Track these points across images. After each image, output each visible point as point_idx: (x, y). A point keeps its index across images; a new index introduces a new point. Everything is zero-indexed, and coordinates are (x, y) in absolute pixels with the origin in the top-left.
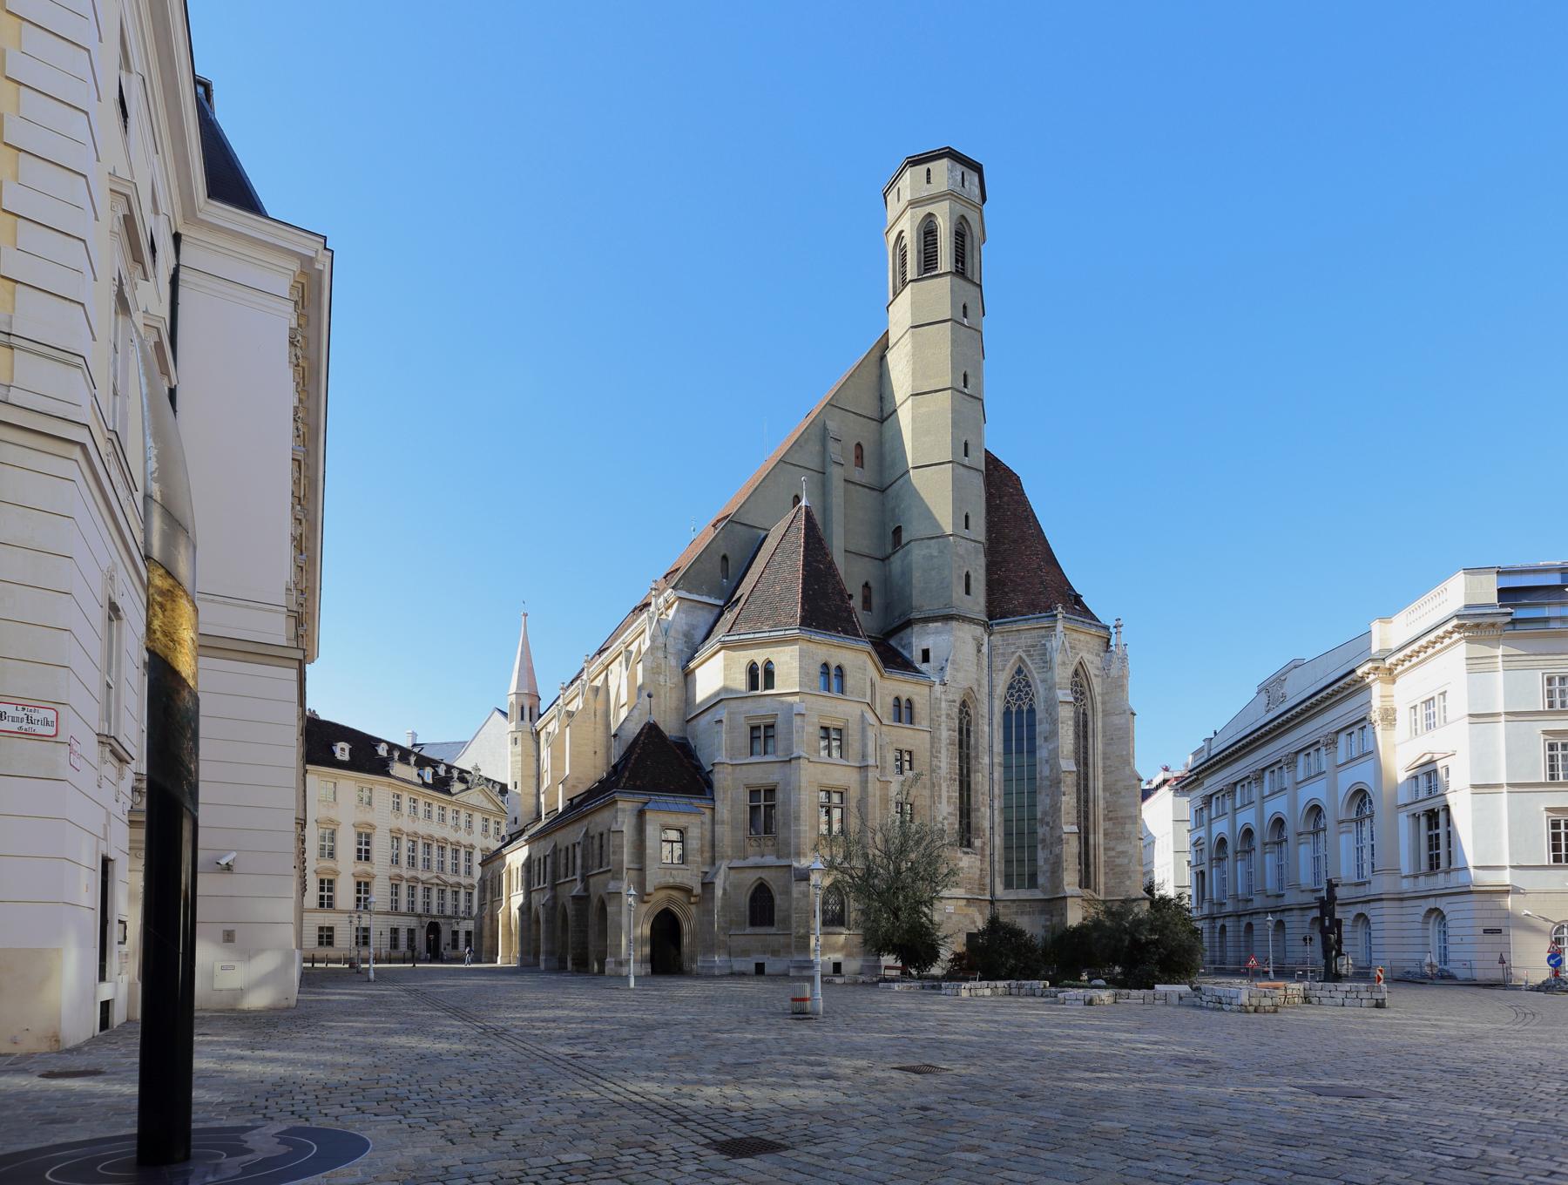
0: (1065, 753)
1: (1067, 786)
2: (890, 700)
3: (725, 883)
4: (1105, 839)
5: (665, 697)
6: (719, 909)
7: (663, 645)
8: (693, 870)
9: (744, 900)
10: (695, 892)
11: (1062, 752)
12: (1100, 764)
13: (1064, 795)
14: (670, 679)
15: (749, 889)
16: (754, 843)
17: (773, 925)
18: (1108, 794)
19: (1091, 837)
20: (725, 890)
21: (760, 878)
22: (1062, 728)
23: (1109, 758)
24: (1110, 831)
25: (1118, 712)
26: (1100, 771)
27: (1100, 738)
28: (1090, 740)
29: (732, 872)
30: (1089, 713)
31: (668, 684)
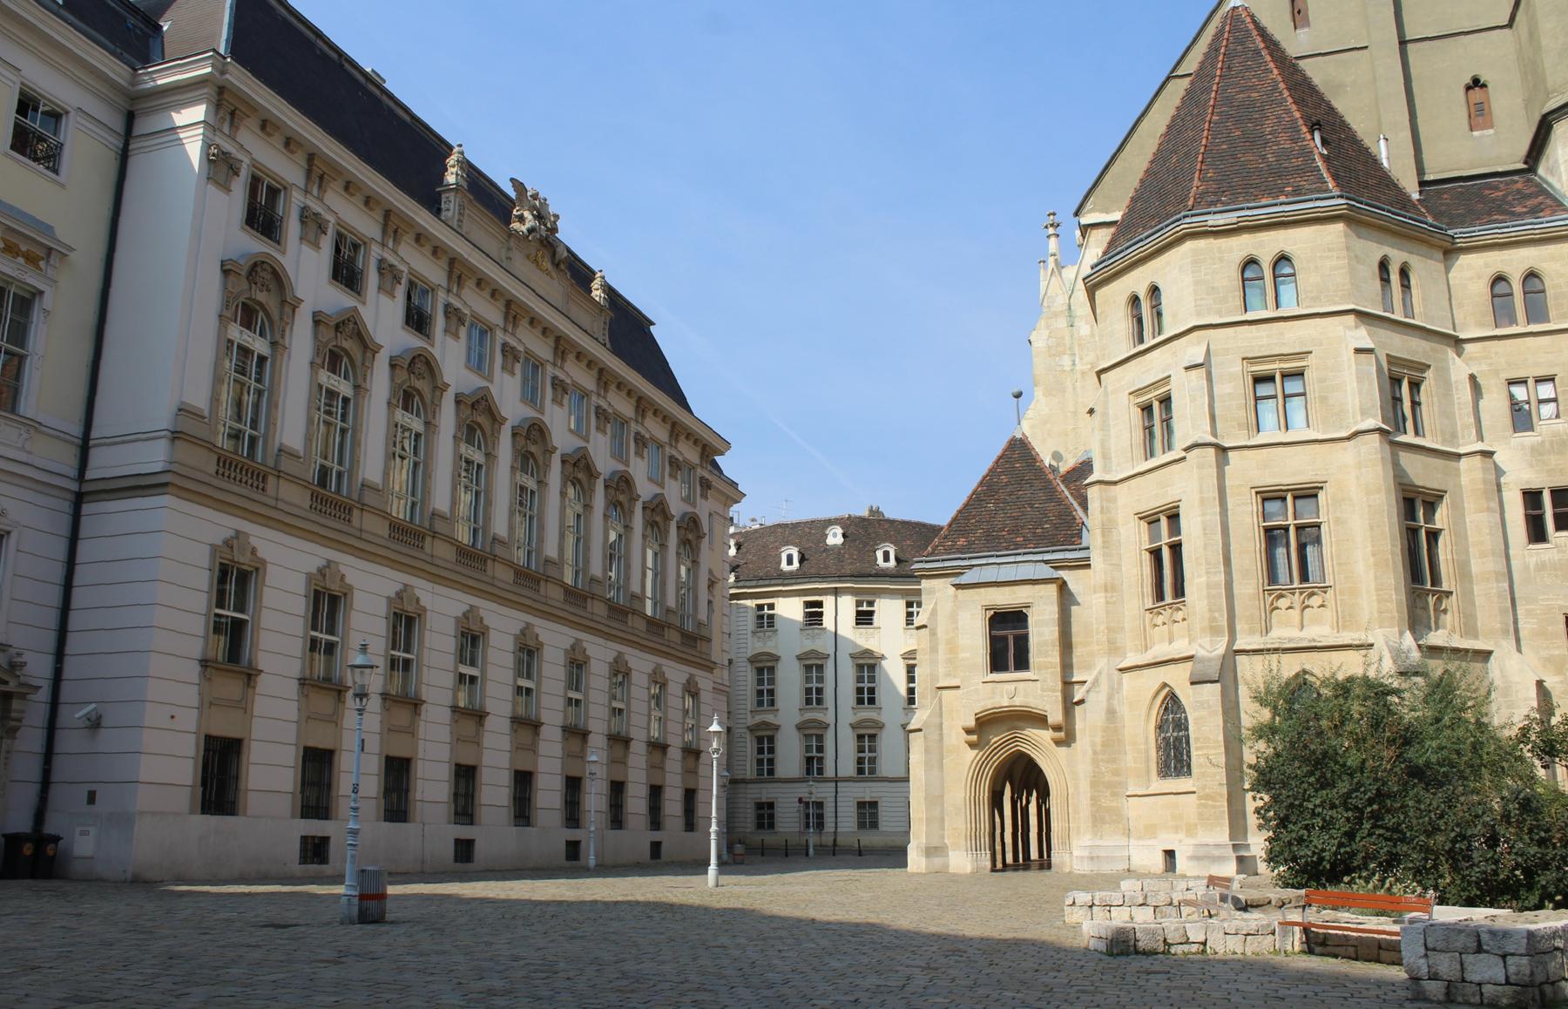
2: (1481, 288)
3: (1110, 698)
5: (1074, 389)
6: (1099, 748)
7: (1066, 307)
8: (1045, 681)
9: (1141, 732)
10: (1050, 720)
14: (1081, 359)
15: (1150, 708)
16: (1159, 620)
17: (1189, 773)
20: (1111, 713)
21: (1165, 685)
29: (1126, 676)
31: (1079, 367)
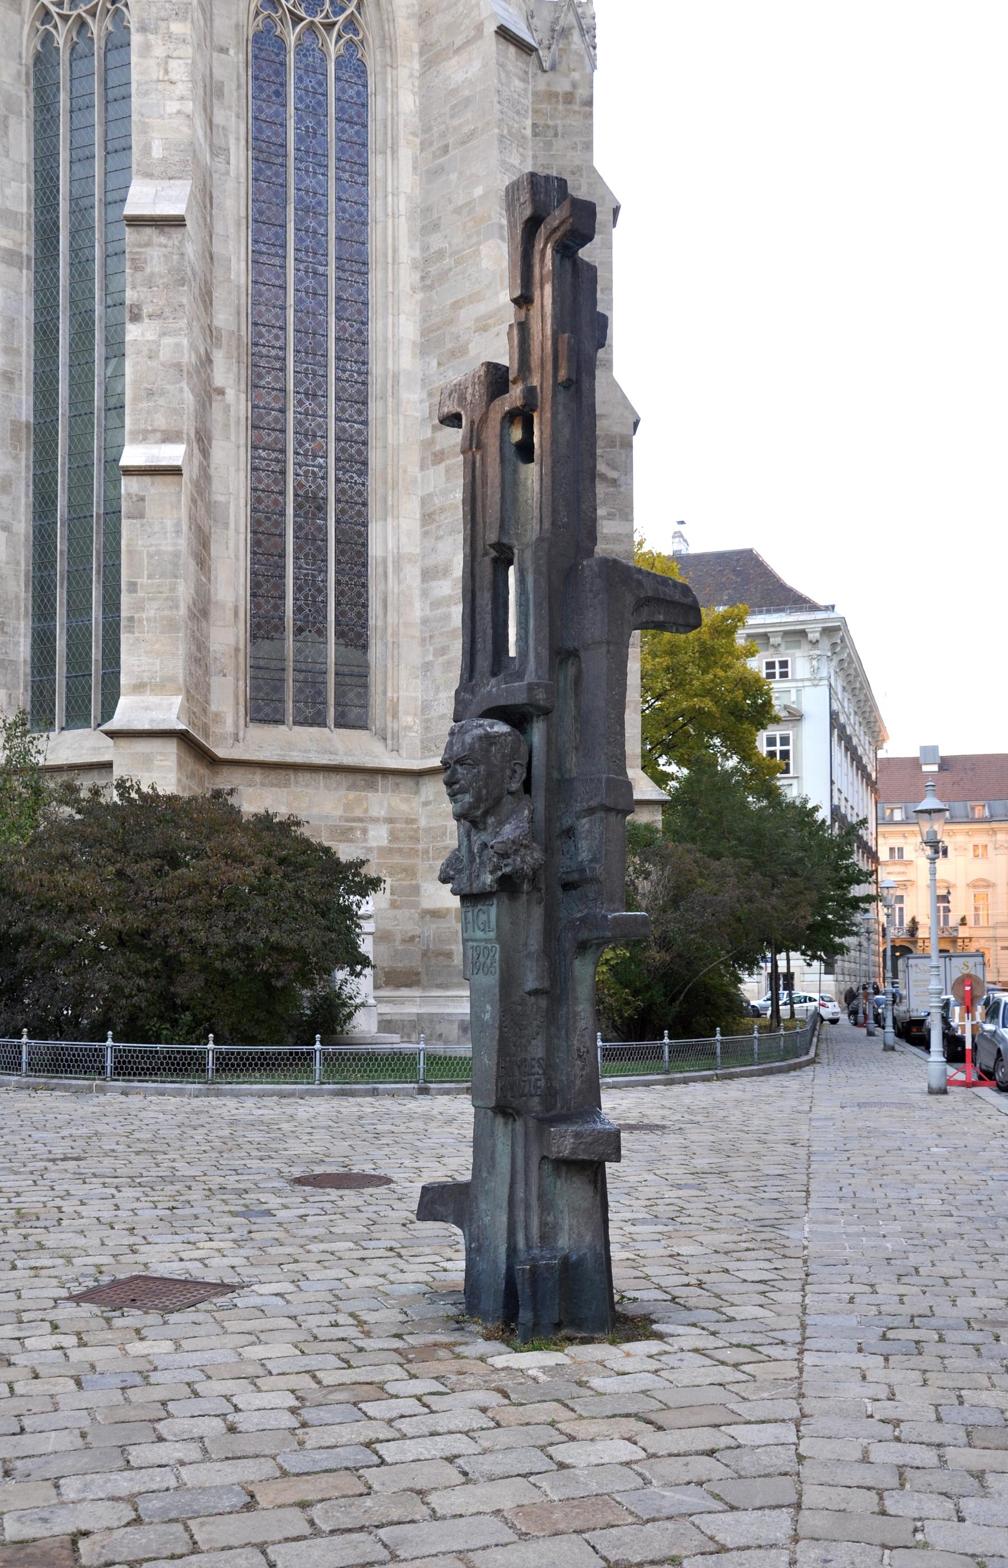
0: (157, 152)
1: (150, 283)
4: (425, 534)
11: (147, 149)
12: (407, 253)
13: (136, 318)
18: (434, 363)
19: (375, 531)
22: (147, 47)
23: (436, 227)
24: (437, 501)
25: (458, 42)
26: (407, 278)
27: (406, 154)
28: (376, 165)
30: (373, 58)
